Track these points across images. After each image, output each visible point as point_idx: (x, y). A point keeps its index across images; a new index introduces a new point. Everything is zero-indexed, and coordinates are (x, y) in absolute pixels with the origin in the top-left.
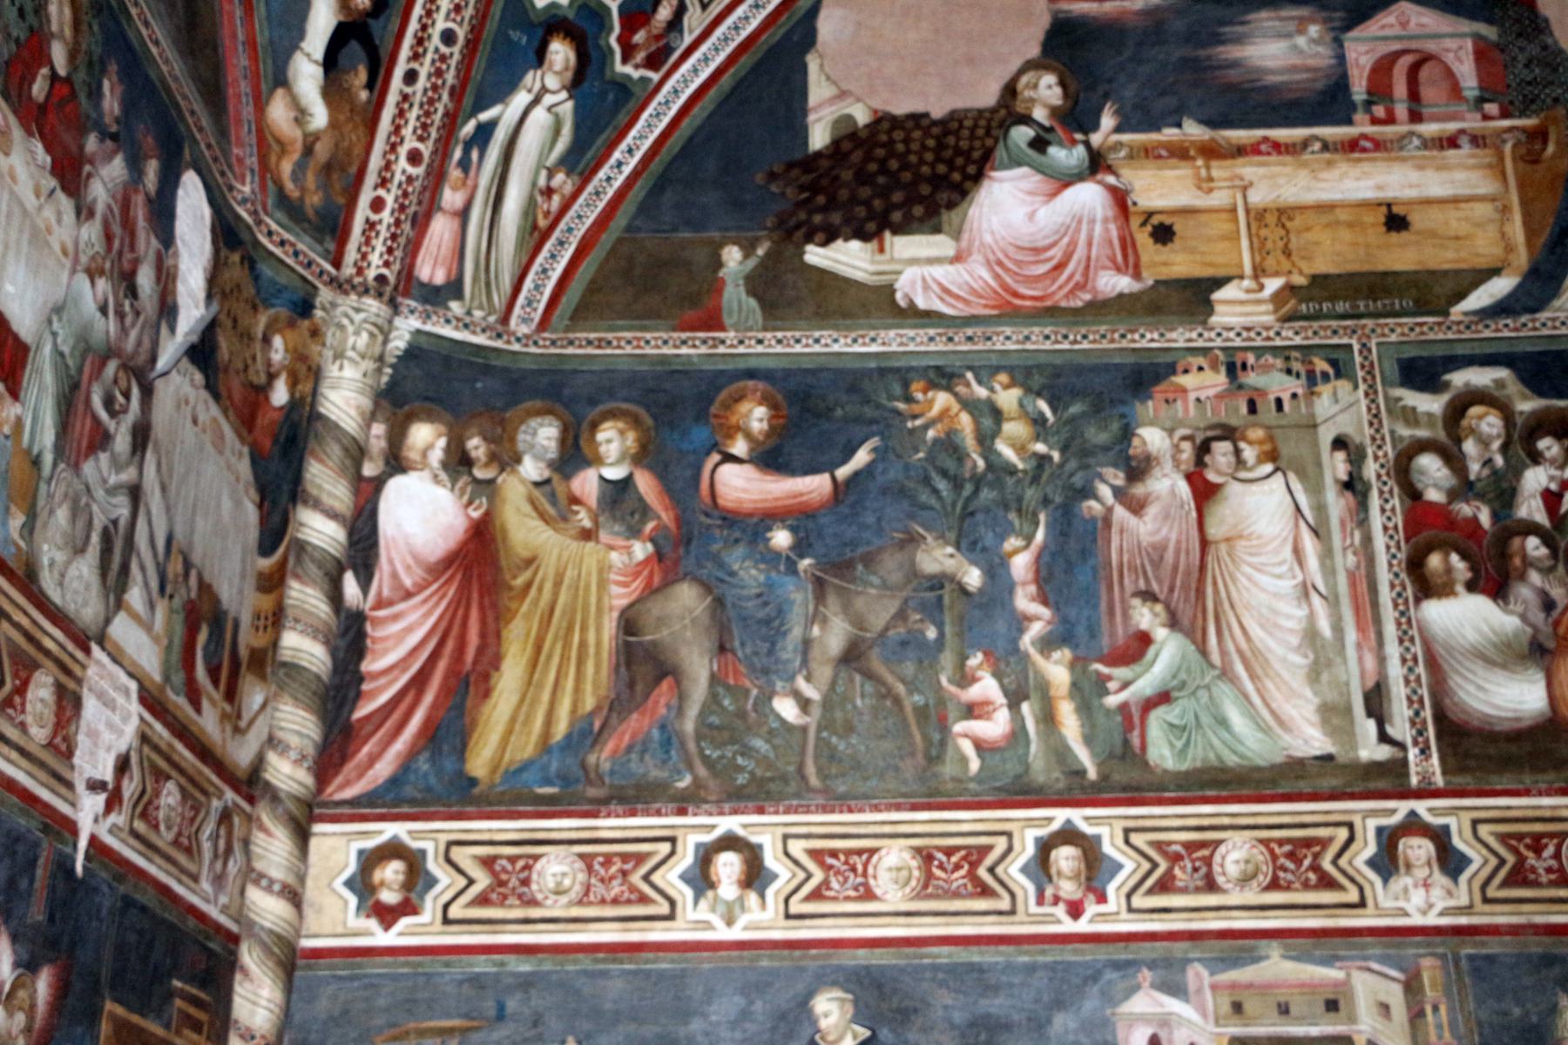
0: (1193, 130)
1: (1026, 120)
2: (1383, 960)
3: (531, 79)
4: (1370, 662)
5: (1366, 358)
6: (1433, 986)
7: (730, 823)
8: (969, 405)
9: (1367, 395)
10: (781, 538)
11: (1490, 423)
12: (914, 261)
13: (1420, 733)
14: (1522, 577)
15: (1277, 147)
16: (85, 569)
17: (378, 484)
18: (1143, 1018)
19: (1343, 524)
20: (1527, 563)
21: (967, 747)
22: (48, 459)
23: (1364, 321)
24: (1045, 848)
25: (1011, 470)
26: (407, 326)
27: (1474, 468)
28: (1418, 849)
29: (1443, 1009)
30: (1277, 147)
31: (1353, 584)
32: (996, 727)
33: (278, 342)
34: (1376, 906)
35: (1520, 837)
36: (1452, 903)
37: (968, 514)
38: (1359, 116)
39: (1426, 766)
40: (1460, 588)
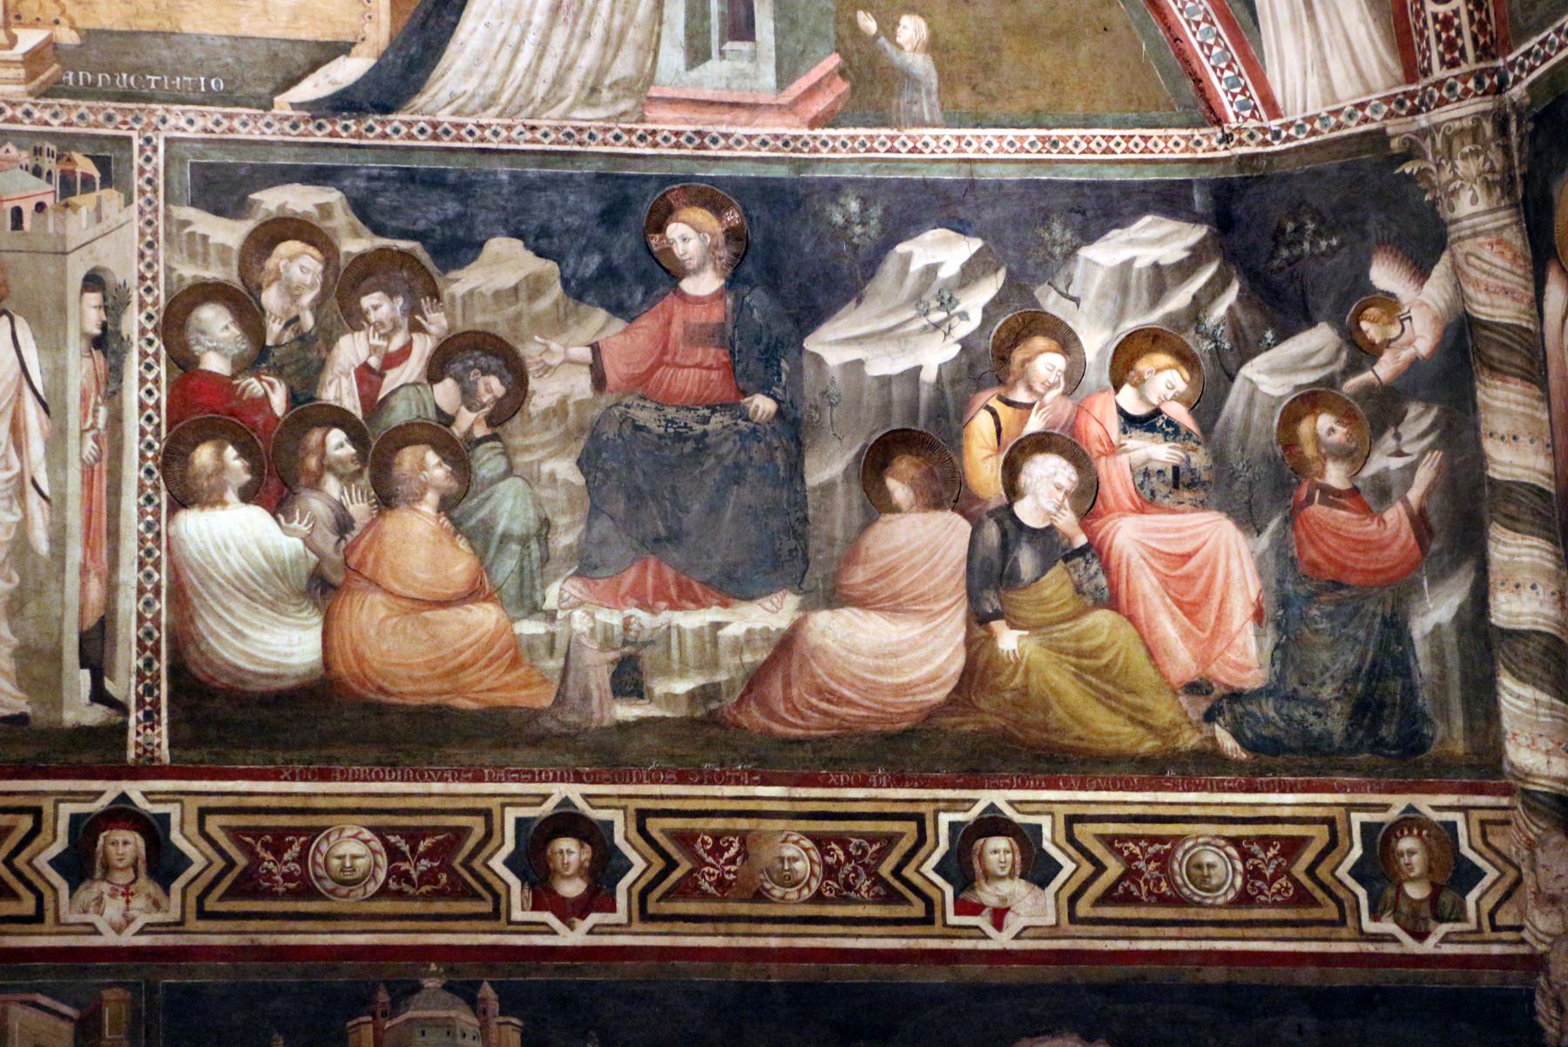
4: (95, 589)
5: (148, 160)
9: (141, 212)
13: (149, 690)
14: (316, 484)
19: (84, 398)
20: (325, 467)
23: (153, 106)
27: (274, 328)
28: (125, 845)
31: (88, 482)
34: (57, 918)
35: (258, 832)
36: (158, 917)
40: (231, 496)
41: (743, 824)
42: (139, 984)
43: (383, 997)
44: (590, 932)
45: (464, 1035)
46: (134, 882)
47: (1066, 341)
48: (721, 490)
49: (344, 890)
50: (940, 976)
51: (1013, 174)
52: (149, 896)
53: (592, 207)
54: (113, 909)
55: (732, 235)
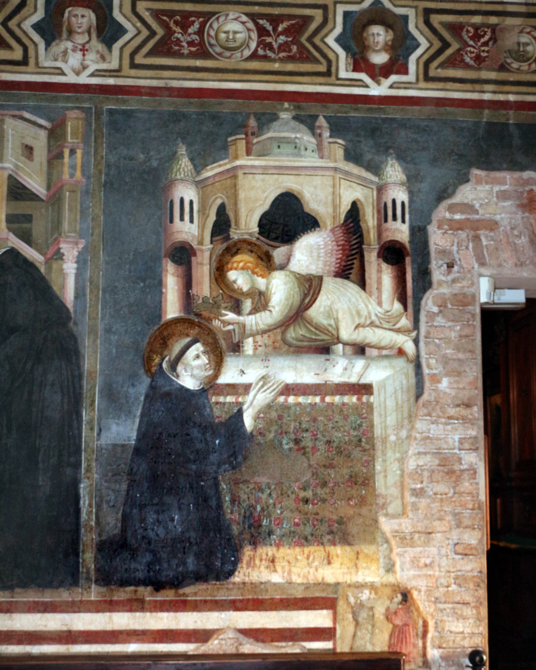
2: (35, 110)
6: (74, 134)
29: (79, 153)
34: (37, 64)
35: (171, 14)
36: (104, 66)
41: (493, 20)
42: (90, 108)
43: (252, 122)
44: (391, 87)
45: (306, 149)
46: (88, 42)
49: (228, 54)
52: (98, 52)
54: (75, 59)
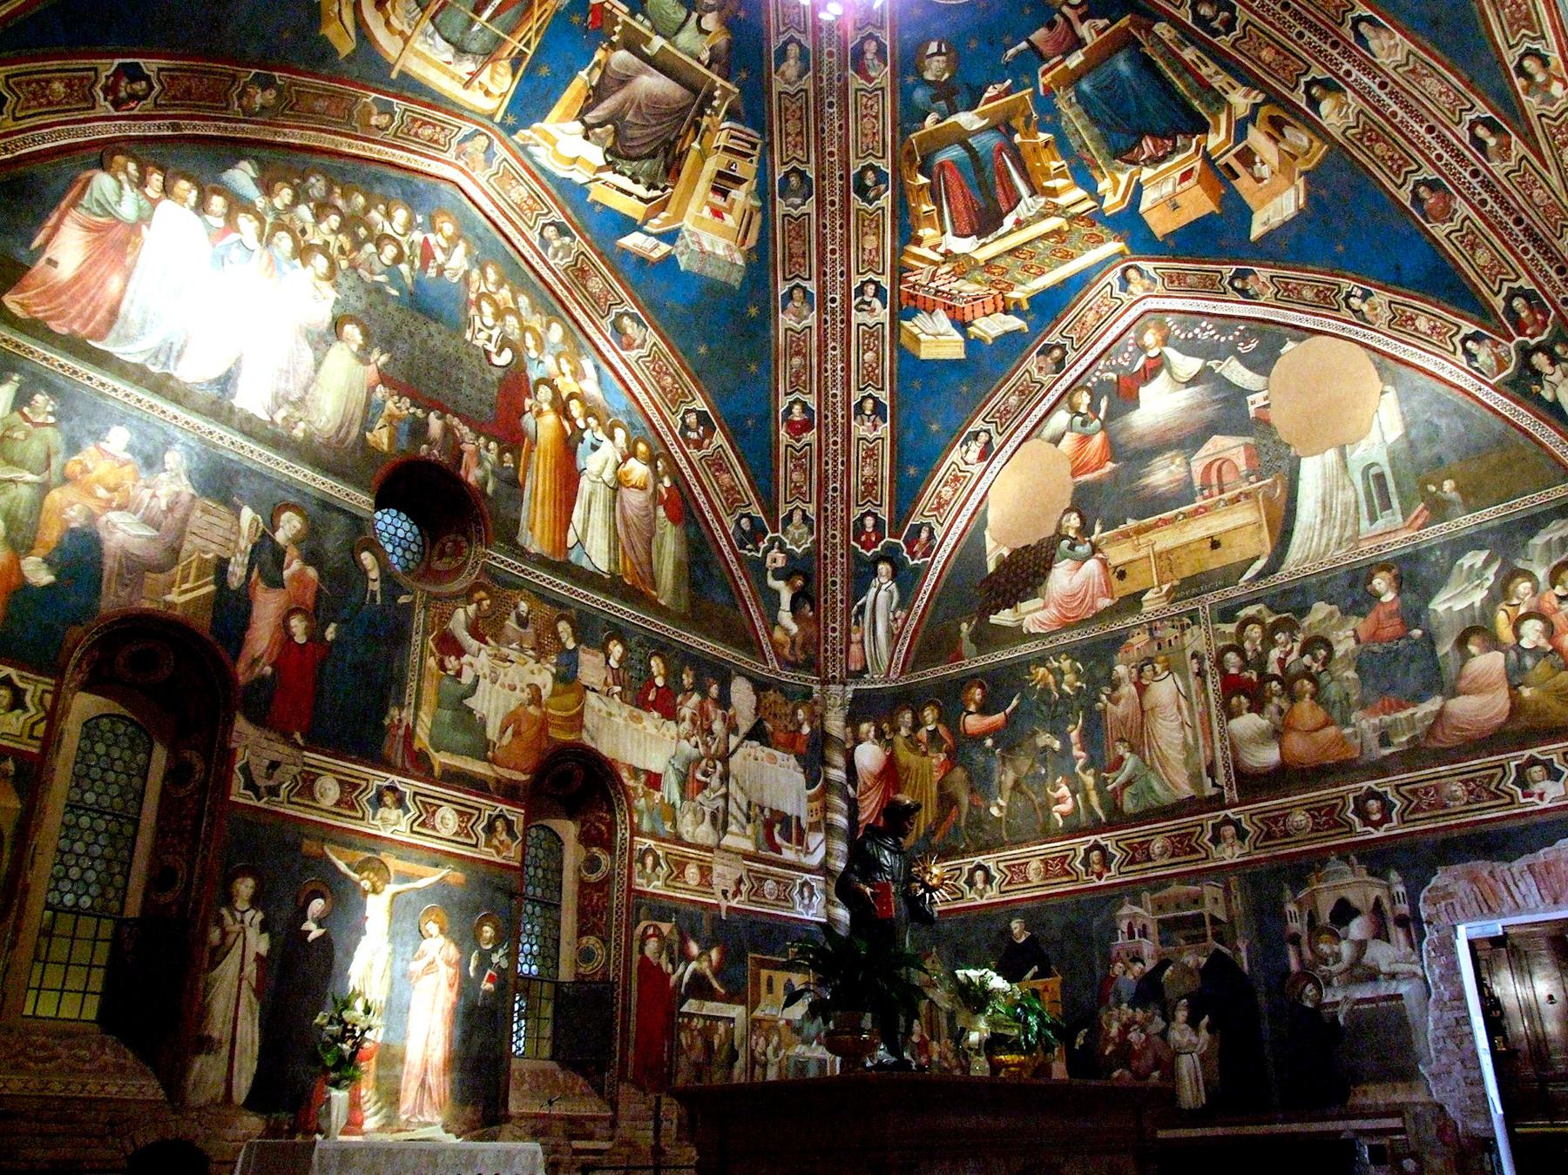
0: (1131, 523)
1: (1067, 537)
3: (875, 582)
7: (979, 859)
8: (1051, 671)
10: (989, 742)
11: (1254, 631)
12: (1029, 612)
15: (1166, 522)
16: (706, 827)
17: (853, 749)
18: (1127, 916)
21: (1058, 816)
22: (678, 803)
24: (1088, 852)
25: (1068, 696)
26: (850, 688)
28: (1229, 830)
30: (1166, 522)
32: (1067, 807)
33: (800, 712)
37: (1054, 718)
38: (1199, 498)
39: (1232, 795)
43: (1317, 866)
47: (1529, 576)
48: (1407, 665)
50: (1522, 822)
51: (1496, 523)
53: (1345, 583)
55: (1395, 577)
